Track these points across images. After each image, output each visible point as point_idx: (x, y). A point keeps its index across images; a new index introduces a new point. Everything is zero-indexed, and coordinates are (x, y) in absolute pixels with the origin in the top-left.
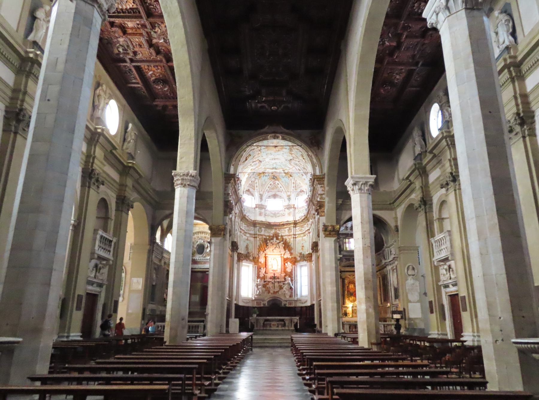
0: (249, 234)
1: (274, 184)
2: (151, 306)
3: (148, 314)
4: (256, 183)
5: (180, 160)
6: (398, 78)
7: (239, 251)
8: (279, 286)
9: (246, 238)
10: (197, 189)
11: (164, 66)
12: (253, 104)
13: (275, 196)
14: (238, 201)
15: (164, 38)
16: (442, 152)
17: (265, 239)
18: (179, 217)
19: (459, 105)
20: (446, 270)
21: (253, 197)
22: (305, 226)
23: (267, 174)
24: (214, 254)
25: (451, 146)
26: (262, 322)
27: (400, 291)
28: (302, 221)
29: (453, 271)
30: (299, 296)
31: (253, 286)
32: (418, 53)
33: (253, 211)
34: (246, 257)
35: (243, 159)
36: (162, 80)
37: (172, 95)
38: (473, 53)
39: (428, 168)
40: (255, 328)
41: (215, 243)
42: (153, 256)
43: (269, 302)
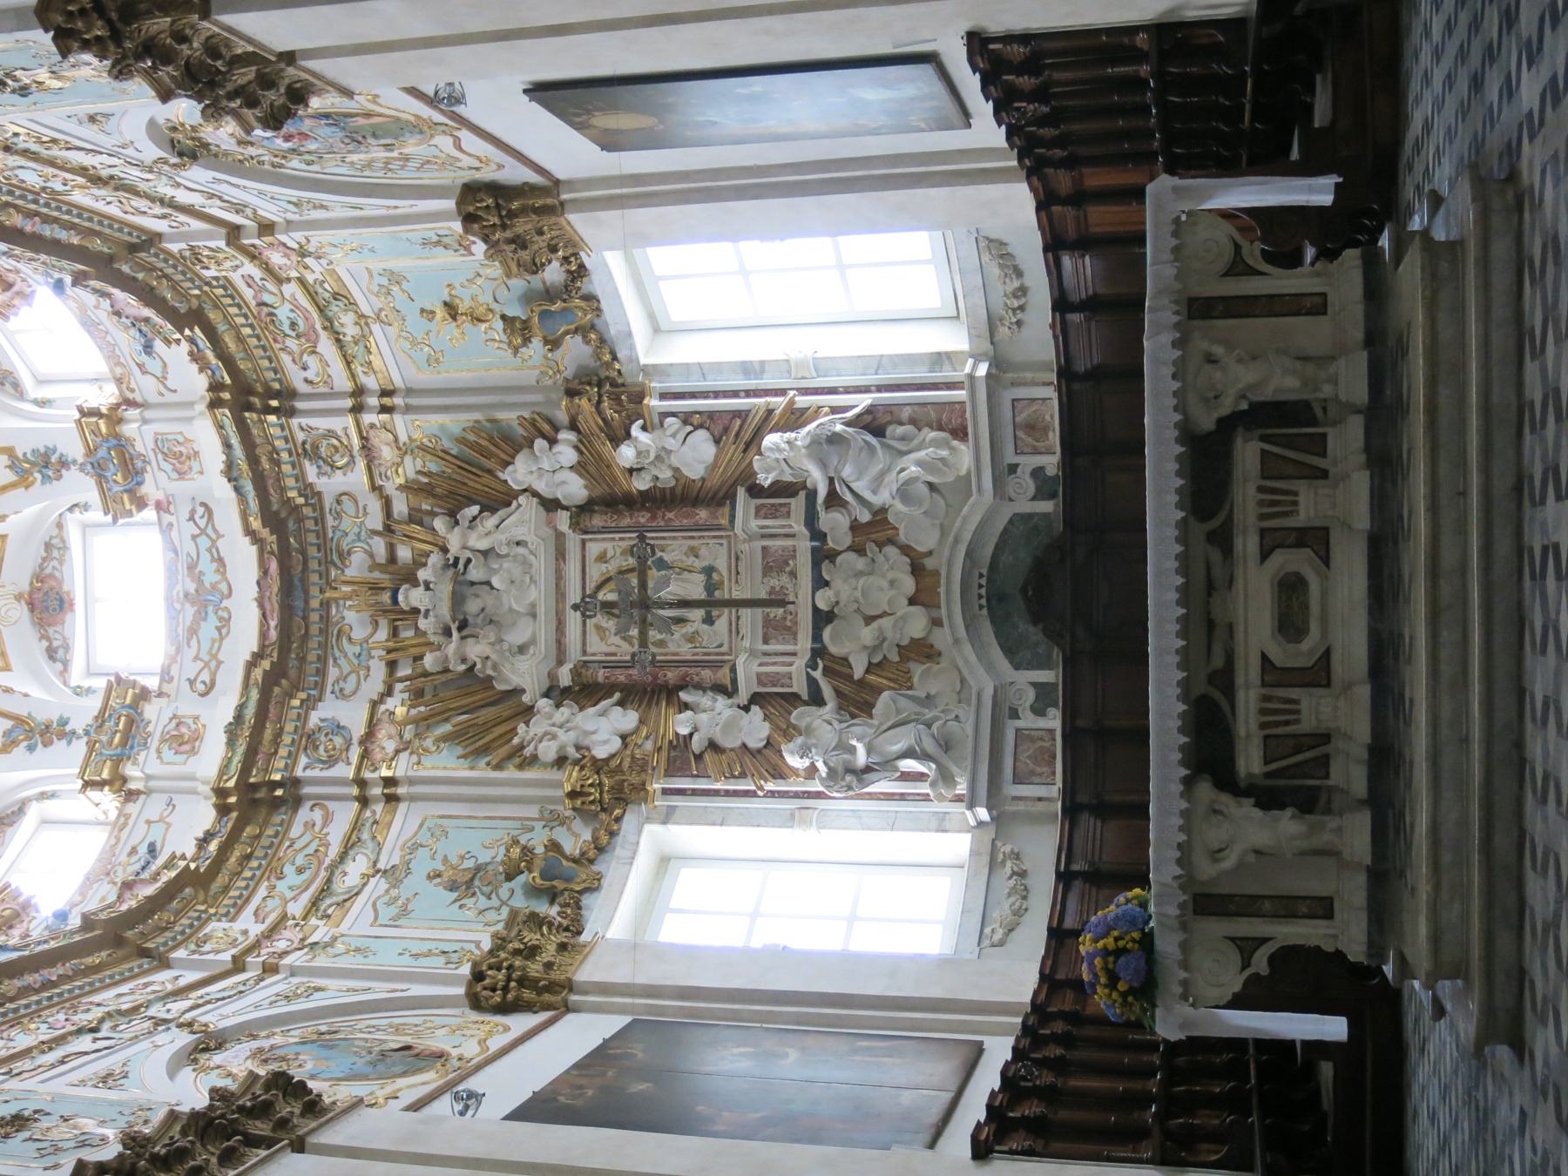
0: (343, 857)
8: (859, 550)
9: (378, 885)
17: (417, 695)
21: (33, 812)
30: (955, 339)
33: (153, 807)
43: (1014, 652)
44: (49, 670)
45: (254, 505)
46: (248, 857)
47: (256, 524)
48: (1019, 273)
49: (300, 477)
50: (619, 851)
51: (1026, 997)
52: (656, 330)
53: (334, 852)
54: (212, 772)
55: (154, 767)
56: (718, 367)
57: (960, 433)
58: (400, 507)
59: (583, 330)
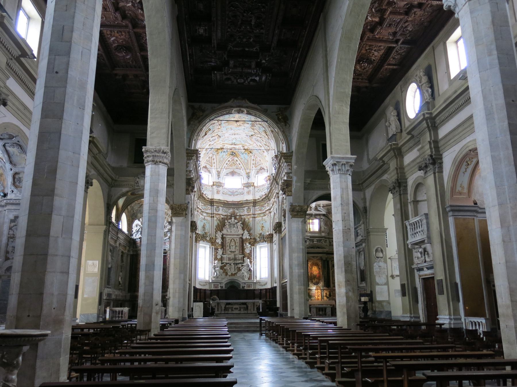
1: (232, 160)
2: (106, 291)
3: (105, 298)
4: (214, 159)
5: (150, 135)
6: (376, 55)
7: (197, 232)
8: (237, 268)
9: (203, 217)
10: (168, 166)
11: (129, 32)
12: (217, 76)
13: (233, 173)
14: (198, 178)
15: (132, 2)
16: (421, 133)
17: (222, 218)
18: (150, 196)
19: (481, 92)
20: (421, 253)
21: (210, 175)
22: (265, 205)
23: (225, 150)
24: (175, 235)
25: (431, 128)
26: (223, 306)
27: (368, 273)
28: (262, 200)
29: (428, 254)
30: (258, 279)
31: (210, 268)
32: (399, 30)
33: (211, 189)
34: (203, 237)
35: (202, 133)
36: (125, 47)
37: (134, 64)
38: (496, 39)
39: (404, 149)
40: (216, 312)
41: (176, 223)
42: (109, 237)
43: (226, 284)
45: (243, 202)
47: (241, 202)
49: (246, 207)
52: (260, 247)
53: (207, 211)
54: (215, 198)
55: (215, 189)
56: (256, 254)
57: (249, 279)
58: (243, 217)
59: (260, 241)
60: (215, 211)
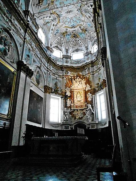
0: (58, 75)
4: (62, 41)
13: (77, 50)
21: (61, 52)
30: (100, 120)
34: (56, 92)
44: (72, 51)
46: (57, 68)
47: (83, 65)
48: (104, 125)
49: (87, 68)
50: (59, 96)
51: (46, 128)
52: (100, 95)
53: (58, 74)
55: (65, 60)
57: (92, 121)
59: (99, 89)
60: (64, 73)
